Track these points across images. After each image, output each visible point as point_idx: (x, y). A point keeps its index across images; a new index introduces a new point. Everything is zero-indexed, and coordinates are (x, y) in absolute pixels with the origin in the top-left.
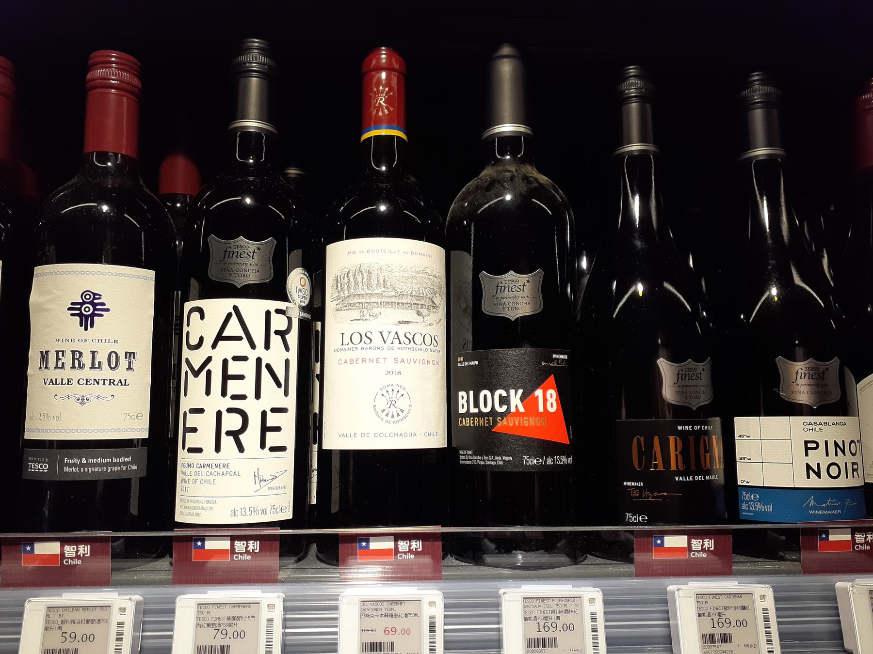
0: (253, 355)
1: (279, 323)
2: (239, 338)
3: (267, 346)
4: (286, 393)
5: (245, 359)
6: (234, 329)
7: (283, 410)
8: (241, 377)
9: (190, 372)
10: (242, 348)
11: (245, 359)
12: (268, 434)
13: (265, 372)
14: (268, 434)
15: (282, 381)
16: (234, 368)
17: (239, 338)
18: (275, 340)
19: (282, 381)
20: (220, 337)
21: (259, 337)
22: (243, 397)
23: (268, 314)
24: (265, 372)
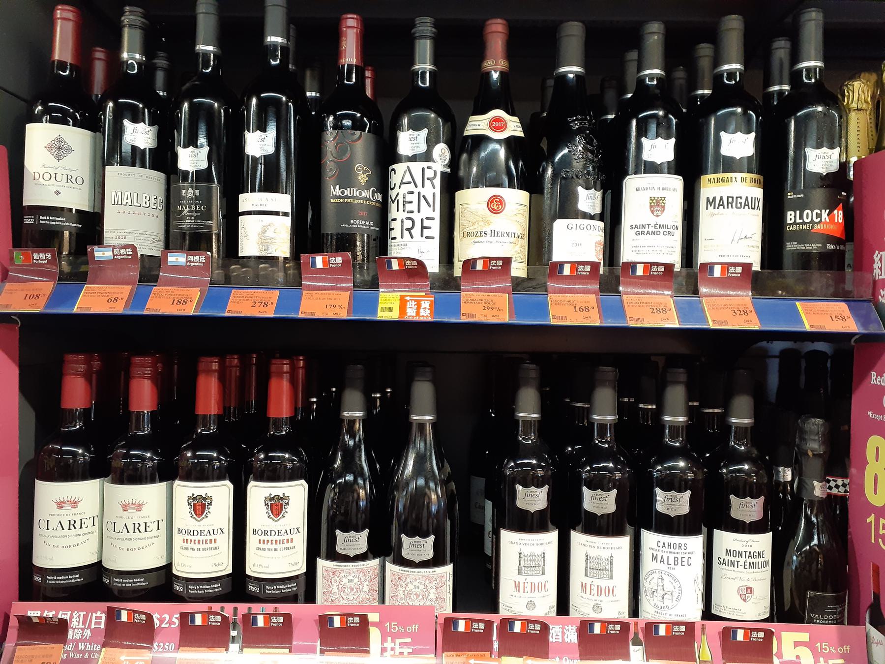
0: (416, 191)
1: (429, 174)
2: (409, 183)
3: (423, 186)
4: (434, 210)
5: (412, 193)
6: (408, 178)
7: (433, 219)
8: (411, 202)
9: (391, 202)
10: (411, 187)
11: (412, 193)
12: (424, 230)
13: (422, 199)
14: (424, 230)
15: (432, 204)
16: (409, 198)
17: (409, 183)
18: (427, 182)
19: (432, 204)
20: (402, 183)
21: (419, 182)
22: (412, 212)
23: (423, 169)
24: (422, 199)
